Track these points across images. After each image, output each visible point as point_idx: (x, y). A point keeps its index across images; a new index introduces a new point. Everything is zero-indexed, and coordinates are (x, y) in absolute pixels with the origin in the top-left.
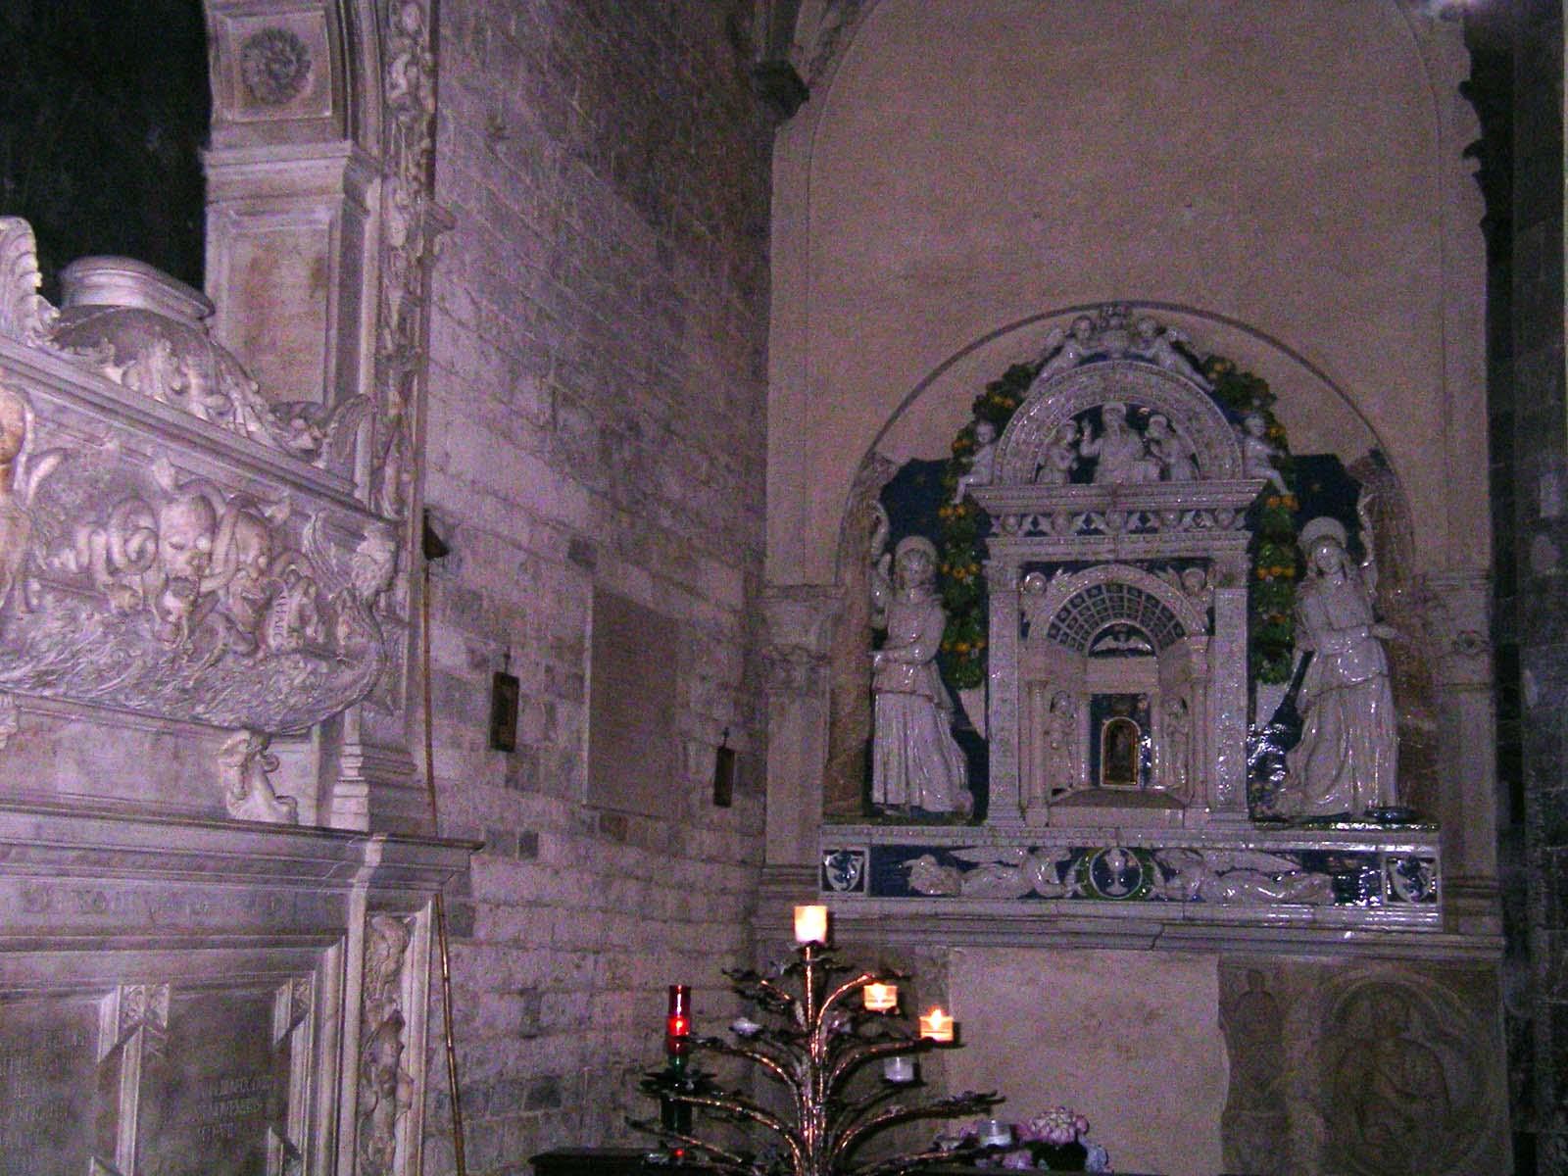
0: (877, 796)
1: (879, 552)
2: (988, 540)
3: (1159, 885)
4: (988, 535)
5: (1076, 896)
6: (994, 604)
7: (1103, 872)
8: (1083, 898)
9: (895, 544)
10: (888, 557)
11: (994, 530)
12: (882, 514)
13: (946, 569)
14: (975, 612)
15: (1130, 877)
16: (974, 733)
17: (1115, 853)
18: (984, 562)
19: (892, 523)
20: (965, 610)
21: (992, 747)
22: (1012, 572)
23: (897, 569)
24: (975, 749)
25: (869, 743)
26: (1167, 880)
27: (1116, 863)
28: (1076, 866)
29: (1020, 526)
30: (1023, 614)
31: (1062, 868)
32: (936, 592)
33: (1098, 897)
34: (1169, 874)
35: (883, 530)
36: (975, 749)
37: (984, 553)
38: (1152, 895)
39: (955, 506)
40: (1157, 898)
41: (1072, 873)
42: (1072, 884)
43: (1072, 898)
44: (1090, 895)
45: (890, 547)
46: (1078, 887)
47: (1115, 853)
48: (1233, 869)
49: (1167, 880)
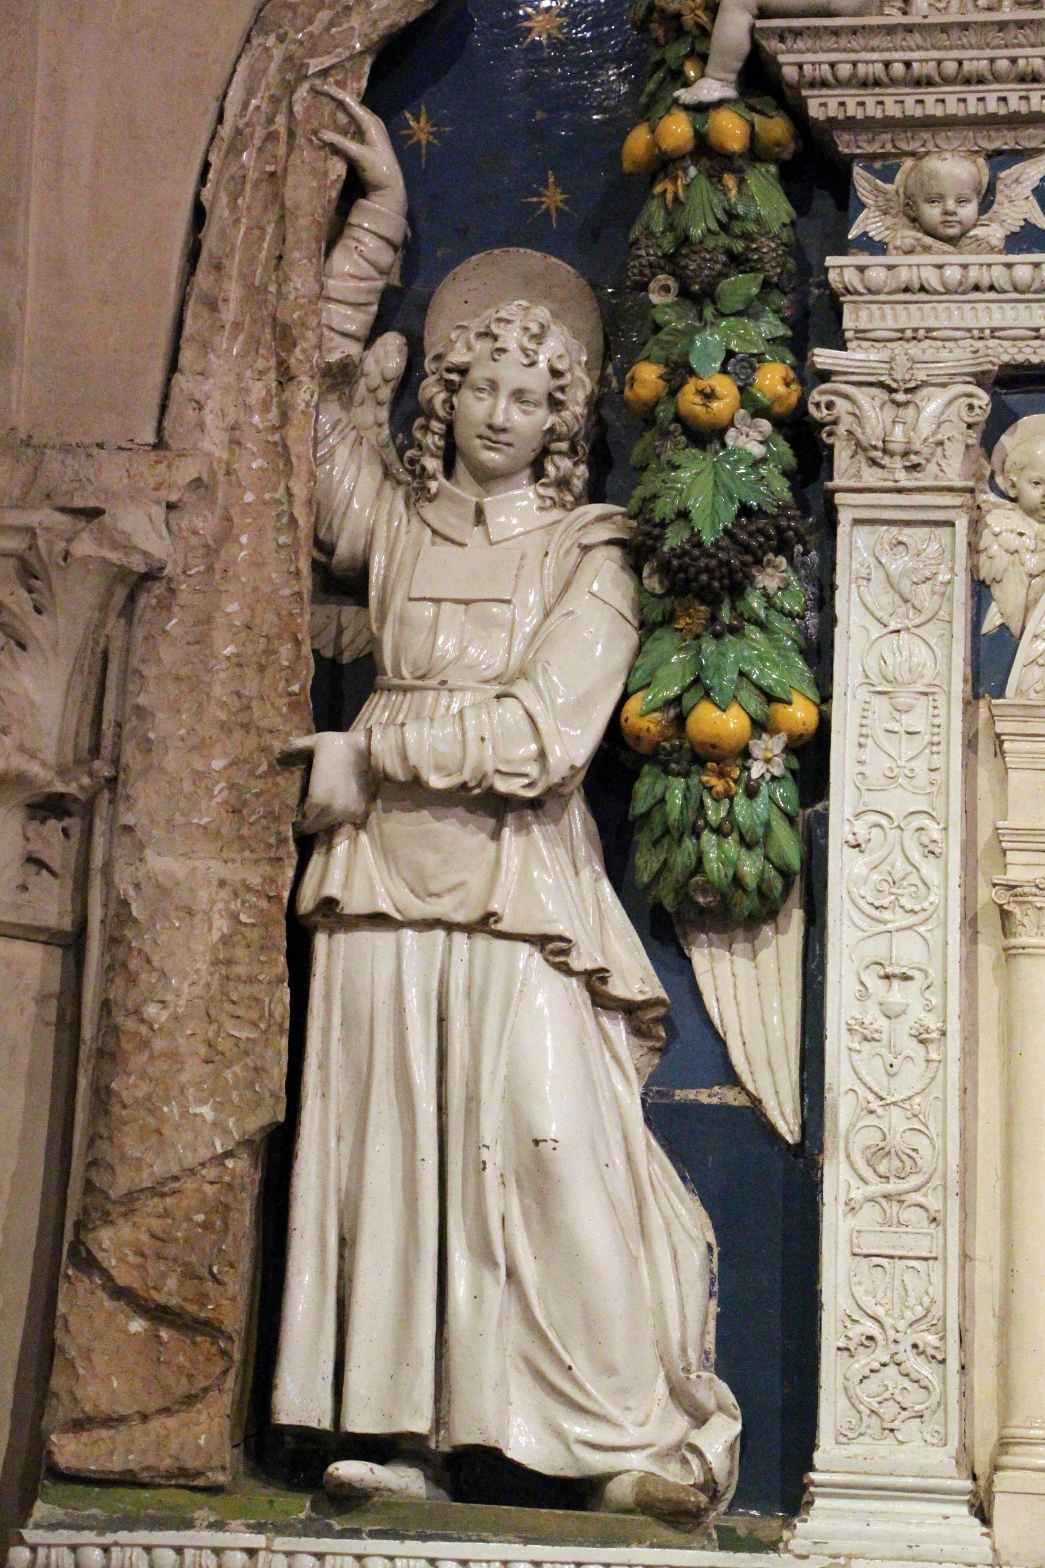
0: (300, 1399)
1: (357, 321)
2: (841, 269)
4: (842, 248)
6: (855, 549)
9: (423, 308)
10: (389, 354)
11: (868, 223)
12: (379, 157)
13: (648, 377)
14: (773, 578)
16: (754, 1113)
18: (823, 357)
19: (410, 217)
20: (729, 567)
21: (839, 1181)
22: (943, 413)
23: (431, 391)
24: (758, 1191)
25: (278, 1149)
29: (987, 200)
30: (981, 592)
32: (595, 493)
35: (382, 215)
36: (758, 1191)
37: (816, 320)
39: (700, 109)
45: (400, 308)
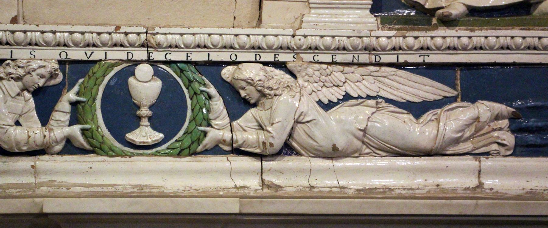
3: (219, 130)
5: (70, 147)
7: (121, 111)
8: (82, 151)
15: (168, 113)
17: (144, 71)
26: (234, 116)
27: (146, 87)
28: (71, 95)
31: (45, 99)
33: (111, 153)
34: (238, 103)
38: (208, 142)
40: (216, 150)
41: (64, 105)
42: (61, 127)
43: (61, 153)
44: (95, 148)
46: (76, 130)
47: (144, 71)
48: (347, 97)
49: (234, 116)
